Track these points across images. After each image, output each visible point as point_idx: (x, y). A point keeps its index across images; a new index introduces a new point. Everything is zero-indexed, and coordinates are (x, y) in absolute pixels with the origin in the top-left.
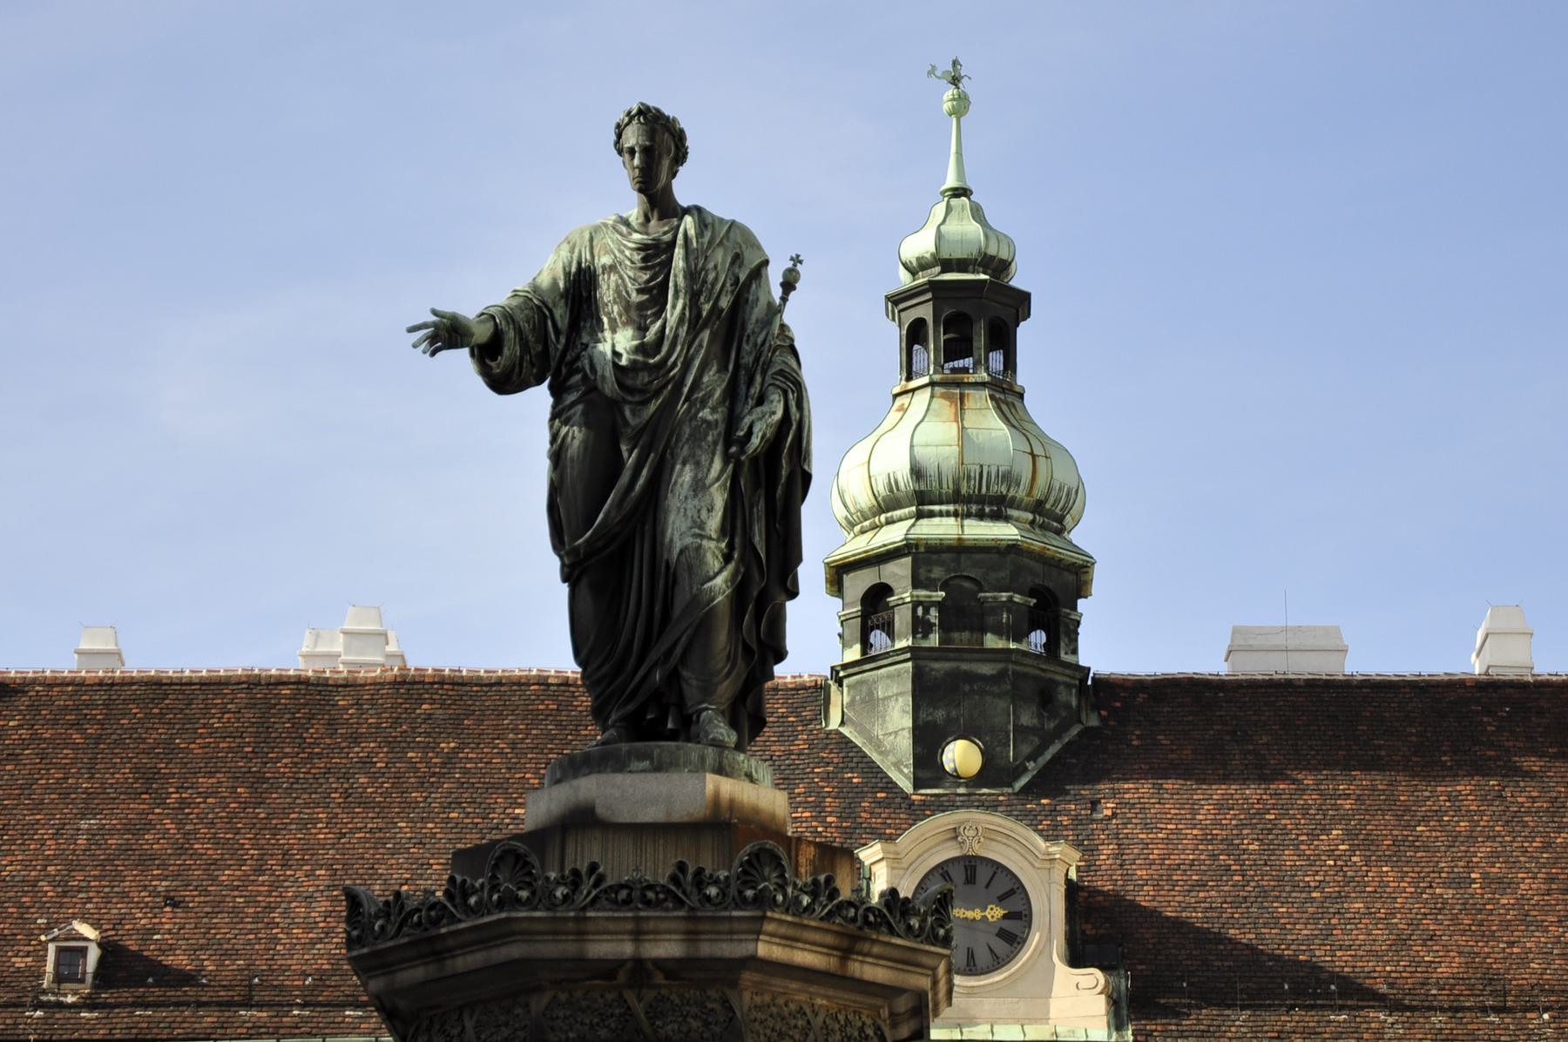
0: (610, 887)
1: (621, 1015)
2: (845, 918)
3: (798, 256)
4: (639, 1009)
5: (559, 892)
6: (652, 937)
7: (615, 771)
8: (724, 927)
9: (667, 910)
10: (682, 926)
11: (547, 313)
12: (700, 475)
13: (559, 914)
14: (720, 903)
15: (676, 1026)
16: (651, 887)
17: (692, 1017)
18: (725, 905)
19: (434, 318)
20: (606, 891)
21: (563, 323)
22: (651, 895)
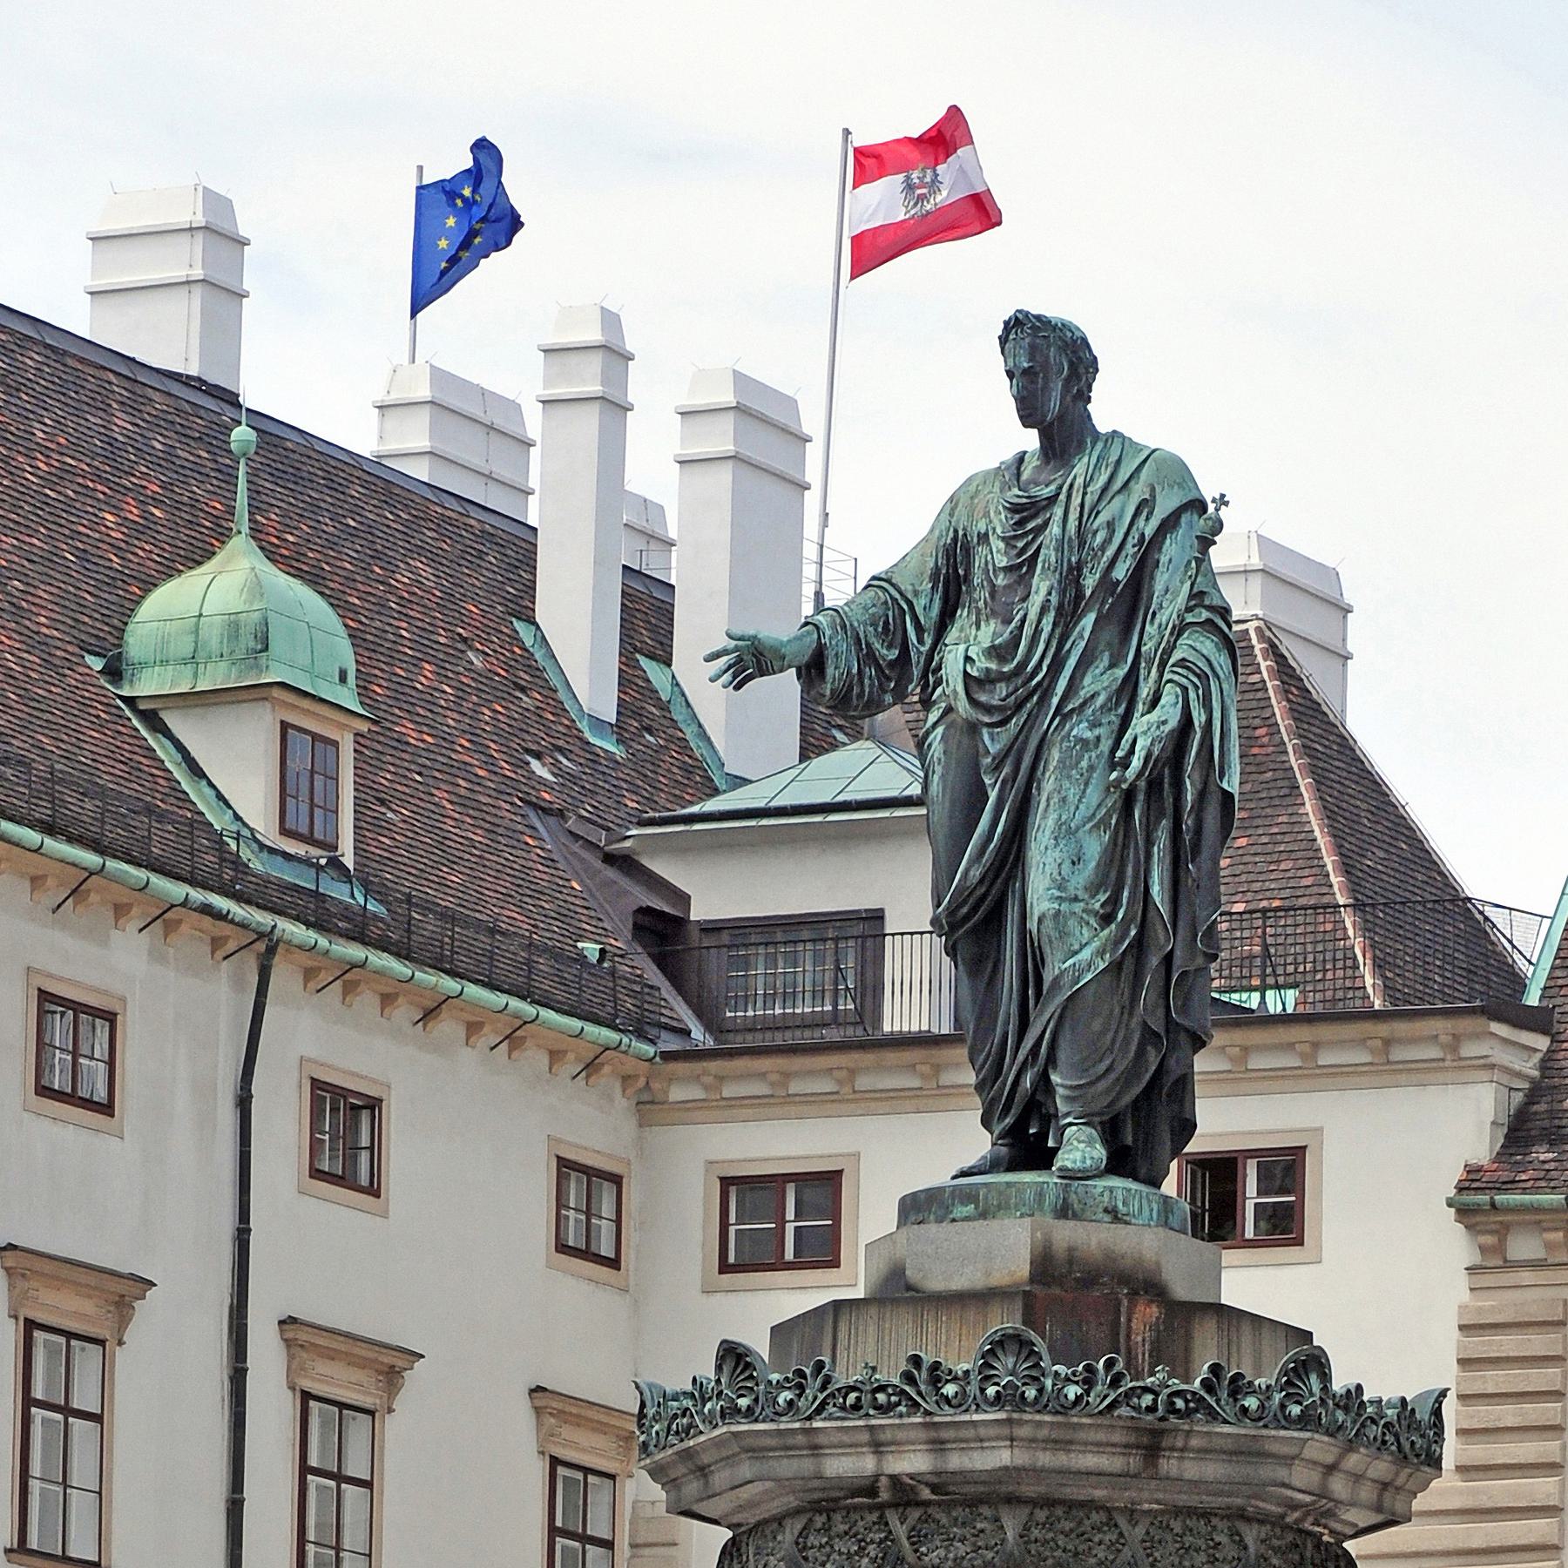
0: (839, 1390)
1: (881, 1541)
2: (1137, 1408)
3: (1223, 496)
4: (901, 1531)
5: (785, 1396)
6: (893, 1448)
7: (940, 1221)
8: (970, 1433)
9: (901, 1416)
10: (922, 1435)
11: (905, 607)
12: (1064, 818)
13: (782, 1426)
14: (960, 1405)
15: (942, 1552)
16: (882, 1389)
17: (960, 1541)
18: (964, 1408)
19: (733, 643)
20: (832, 1395)
21: (930, 617)
22: (881, 1397)
